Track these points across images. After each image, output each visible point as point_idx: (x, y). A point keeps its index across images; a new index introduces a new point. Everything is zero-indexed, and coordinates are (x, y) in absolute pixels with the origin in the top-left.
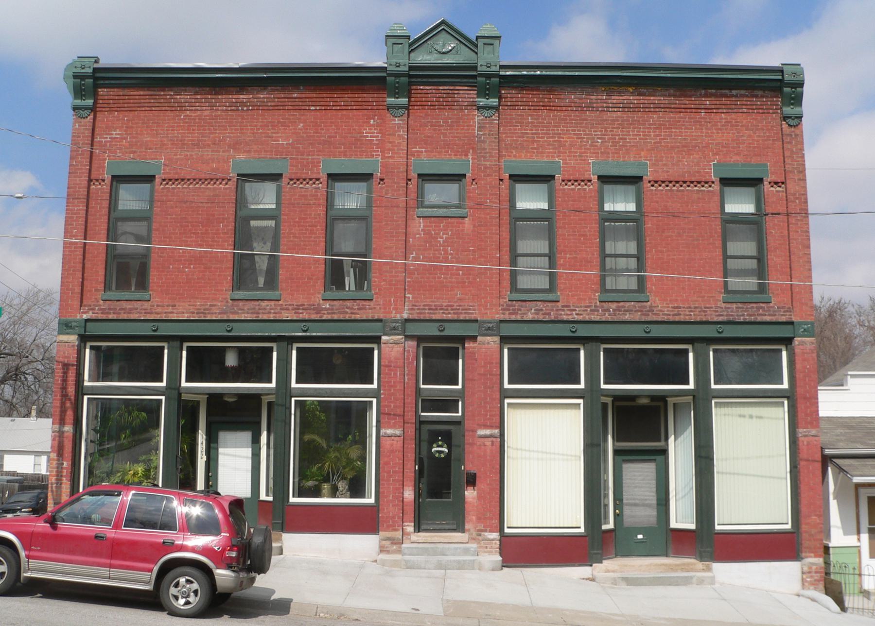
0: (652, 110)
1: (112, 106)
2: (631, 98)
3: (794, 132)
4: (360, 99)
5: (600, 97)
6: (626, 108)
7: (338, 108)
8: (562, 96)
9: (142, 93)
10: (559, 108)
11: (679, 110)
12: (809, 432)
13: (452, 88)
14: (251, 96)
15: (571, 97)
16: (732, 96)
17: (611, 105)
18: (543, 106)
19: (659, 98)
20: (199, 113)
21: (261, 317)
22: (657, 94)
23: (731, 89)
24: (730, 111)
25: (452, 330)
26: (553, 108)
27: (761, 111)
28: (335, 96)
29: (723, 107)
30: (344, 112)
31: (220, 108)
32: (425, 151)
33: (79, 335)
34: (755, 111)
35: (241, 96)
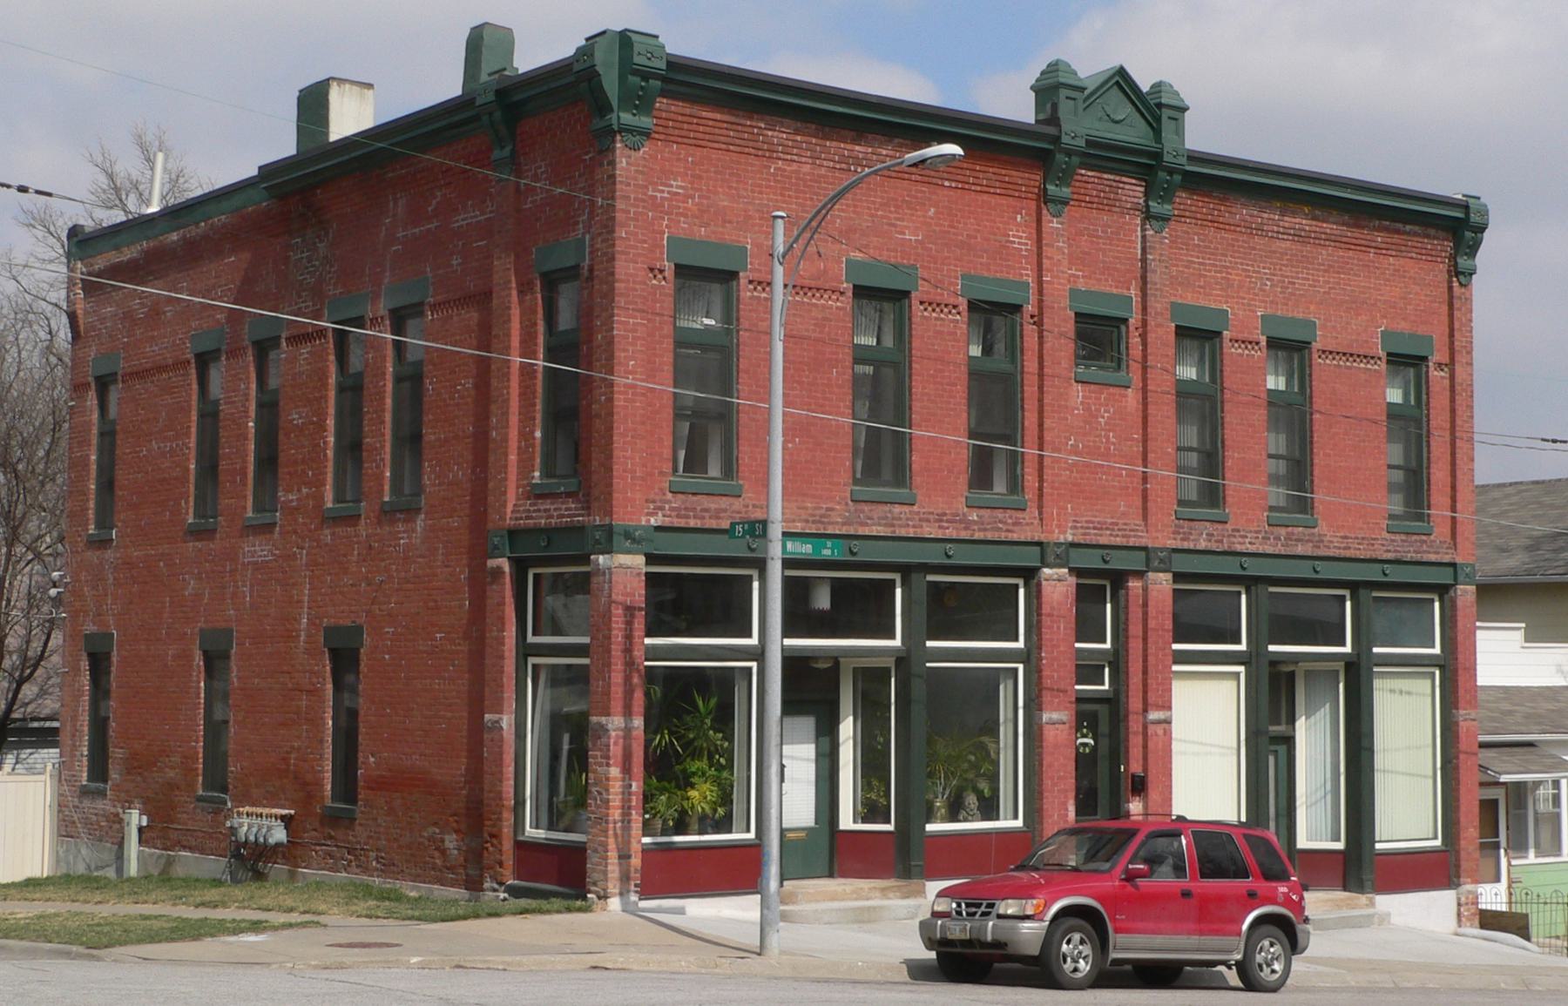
0: (1322, 242)
1: (671, 131)
2: (1304, 222)
3: (1464, 293)
4: (1007, 179)
5: (1272, 216)
6: (1300, 237)
7: (979, 188)
8: (1234, 210)
9: (718, 116)
10: (1227, 227)
11: (1349, 245)
12: (1469, 714)
13: (1118, 178)
14: (870, 150)
15: (1244, 212)
16: (1404, 233)
17: (1281, 230)
18: (1211, 221)
19: (1331, 226)
20: (794, 167)
21: (902, 532)
22: (1331, 220)
23: (1405, 223)
24: (1399, 253)
25: (1118, 563)
26: (1221, 226)
27: (1430, 258)
28: (978, 168)
29: (1394, 247)
30: (985, 197)
31: (825, 163)
32: (1083, 277)
33: (646, 555)
34: (1424, 257)
35: (857, 148)
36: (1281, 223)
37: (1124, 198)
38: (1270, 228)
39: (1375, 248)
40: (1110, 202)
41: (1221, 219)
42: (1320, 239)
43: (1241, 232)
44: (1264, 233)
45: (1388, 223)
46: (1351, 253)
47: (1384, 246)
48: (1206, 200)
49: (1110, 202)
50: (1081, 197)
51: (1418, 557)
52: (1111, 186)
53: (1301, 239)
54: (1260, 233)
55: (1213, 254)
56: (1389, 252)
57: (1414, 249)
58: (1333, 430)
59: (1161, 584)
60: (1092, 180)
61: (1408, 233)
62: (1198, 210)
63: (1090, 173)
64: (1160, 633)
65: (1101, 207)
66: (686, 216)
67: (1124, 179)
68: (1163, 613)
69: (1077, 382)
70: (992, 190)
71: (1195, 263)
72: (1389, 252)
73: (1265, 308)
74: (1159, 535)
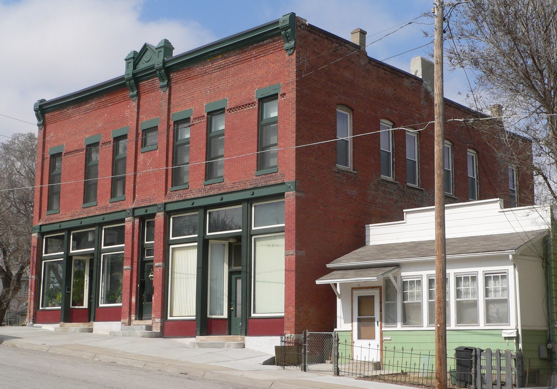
0: (231, 66)
1: (50, 121)
2: (221, 62)
3: (291, 58)
4: (124, 96)
5: (209, 66)
6: (221, 68)
7: (117, 102)
8: (194, 70)
9: (58, 113)
10: (194, 78)
11: (242, 62)
12: (289, 252)
13: (153, 79)
14: (90, 105)
15: (198, 69)
16: (265, 45)
17: (213, 69)
18: (188, 78)
19: (233, 58)
20: (75, 117)
21: (90, 215)
22: (232, 55)
23: (263, 41)
24: (265, 54)
25: (150, 211)
26: (191, 78)
27: (279, 49)
28: (116, 96)
29: (261, 53)
30: (120, 104)
31: (82, 113)
32: (145, 117)
33: (38, 233)
34: (277, 50)
35: (87, 106)
36: (213, 67)
37: (157, 85)
38: (209, 70)
39: (254, 57)
40: (153, 88)
41: (191, 76)
42: (230, 65)
43: (199, 77)
44: (208, 73)
45: (256, 45)
46: (244, 64)
47: (257, 54)
48: (183, 72)
49: (153, 88)
50: (145, 91)
51: (265, 184)
52: (152, 83)
53: (222, 69)
54: (206, 74)
55: (189, 90)
56: (261, 56)
57: (271, 49)
58: (233, 140)
59: (160, 216)
60: (146, 84)
61: (266, 44)
62: (181, 77)
63: (145, 82)
64: (160, 234)
65: (151, 91)
66: (53, 142)
67: (155, 79)
68: (161, 227)
69: (141, 153)
70: (121, 101)
71: (181, 96)
72: (261, 56)
73: (207, 101)
74: (160, 199)
